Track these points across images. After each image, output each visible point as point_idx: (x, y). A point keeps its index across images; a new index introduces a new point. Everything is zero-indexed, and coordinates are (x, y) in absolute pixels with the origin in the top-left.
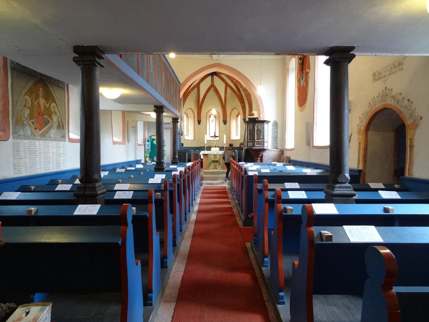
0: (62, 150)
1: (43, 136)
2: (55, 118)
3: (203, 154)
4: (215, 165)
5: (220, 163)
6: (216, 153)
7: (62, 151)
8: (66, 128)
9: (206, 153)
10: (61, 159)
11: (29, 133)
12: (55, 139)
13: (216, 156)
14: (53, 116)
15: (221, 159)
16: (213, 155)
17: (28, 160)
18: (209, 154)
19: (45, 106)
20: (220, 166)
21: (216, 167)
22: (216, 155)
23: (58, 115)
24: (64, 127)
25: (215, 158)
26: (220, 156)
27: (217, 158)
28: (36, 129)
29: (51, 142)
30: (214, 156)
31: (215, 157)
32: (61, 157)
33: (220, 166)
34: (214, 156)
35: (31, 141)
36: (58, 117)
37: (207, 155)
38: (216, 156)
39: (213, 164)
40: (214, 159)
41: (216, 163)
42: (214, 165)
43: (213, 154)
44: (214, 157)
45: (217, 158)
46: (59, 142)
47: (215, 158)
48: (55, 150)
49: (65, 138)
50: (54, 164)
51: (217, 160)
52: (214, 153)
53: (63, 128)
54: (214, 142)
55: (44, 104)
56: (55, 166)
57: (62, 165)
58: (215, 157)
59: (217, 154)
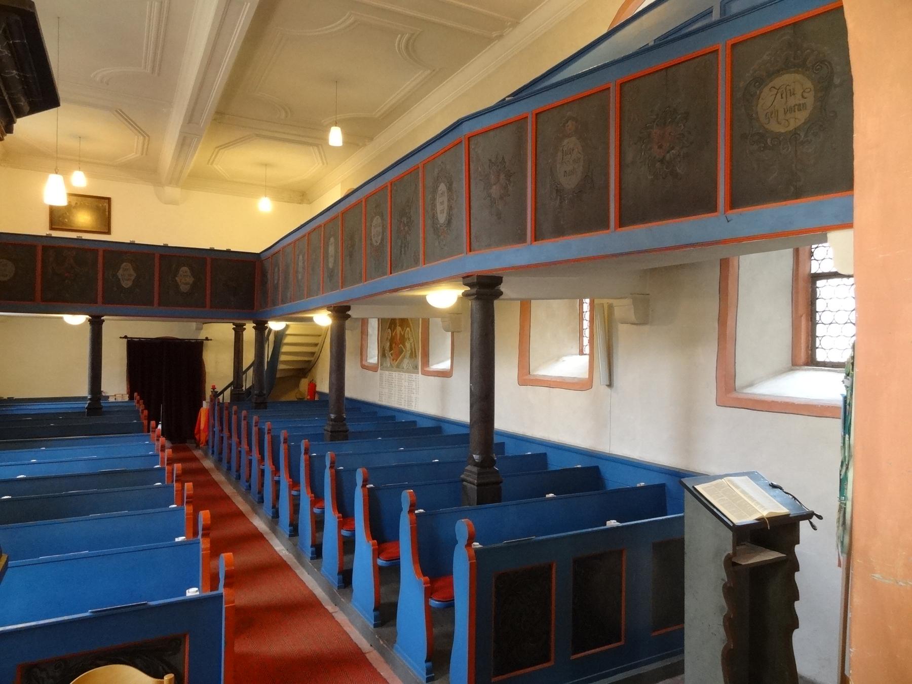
0: (414, 383)
1: (399, 367)
2: (408, 345)
7: (414, 387)
8: (419, 356)
10: (414, 396)
11: (389, 365)
12: (408, 371)
14: (406, 344)
17: (387, 391)
19: (401, 334)
23: (411, 342)
24: (417, 355)
28: (393, 360)
29: (404, 374)
32: (414, 393)
35: (390, 372)
36: (411, 343)
46: (412, 374)
48: (406, 384)
49: (418, 369)
50: (405, 401)
53: (416, 356)
55: (400, 331)
56: (406, 402)
57: (413, 404)
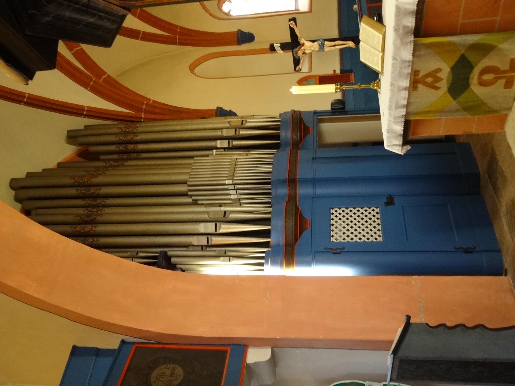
3: (400, 142)
4: (487, 77)
5: (474, 47)
6: (400, 75)
9: (399, 128)
13: (421, 74)
15: (451, 44)
16: (415, 94)
18: (407, 114)
20: (504, 46)
21: (505, 72)
22: (415, 73)
25: (439, 80)
26: (423, 52)
27: (439, 70)
30: (420, 86)
31: (430, 80)
33: (504, 46)
34: (420, 86)
37: (407, 124)
38: (421, 74)
39: (475, 88)
40: (437, 85)
41: (470, 73)
42: (482, 84)
43: (405, 94)
44: (433, 86)
45: (439, 70)
47: (439, 80)
51: (453, 69)
52: (400, 89)
54: (326, 49)
58: (430, 80)
59: (409, 70)
